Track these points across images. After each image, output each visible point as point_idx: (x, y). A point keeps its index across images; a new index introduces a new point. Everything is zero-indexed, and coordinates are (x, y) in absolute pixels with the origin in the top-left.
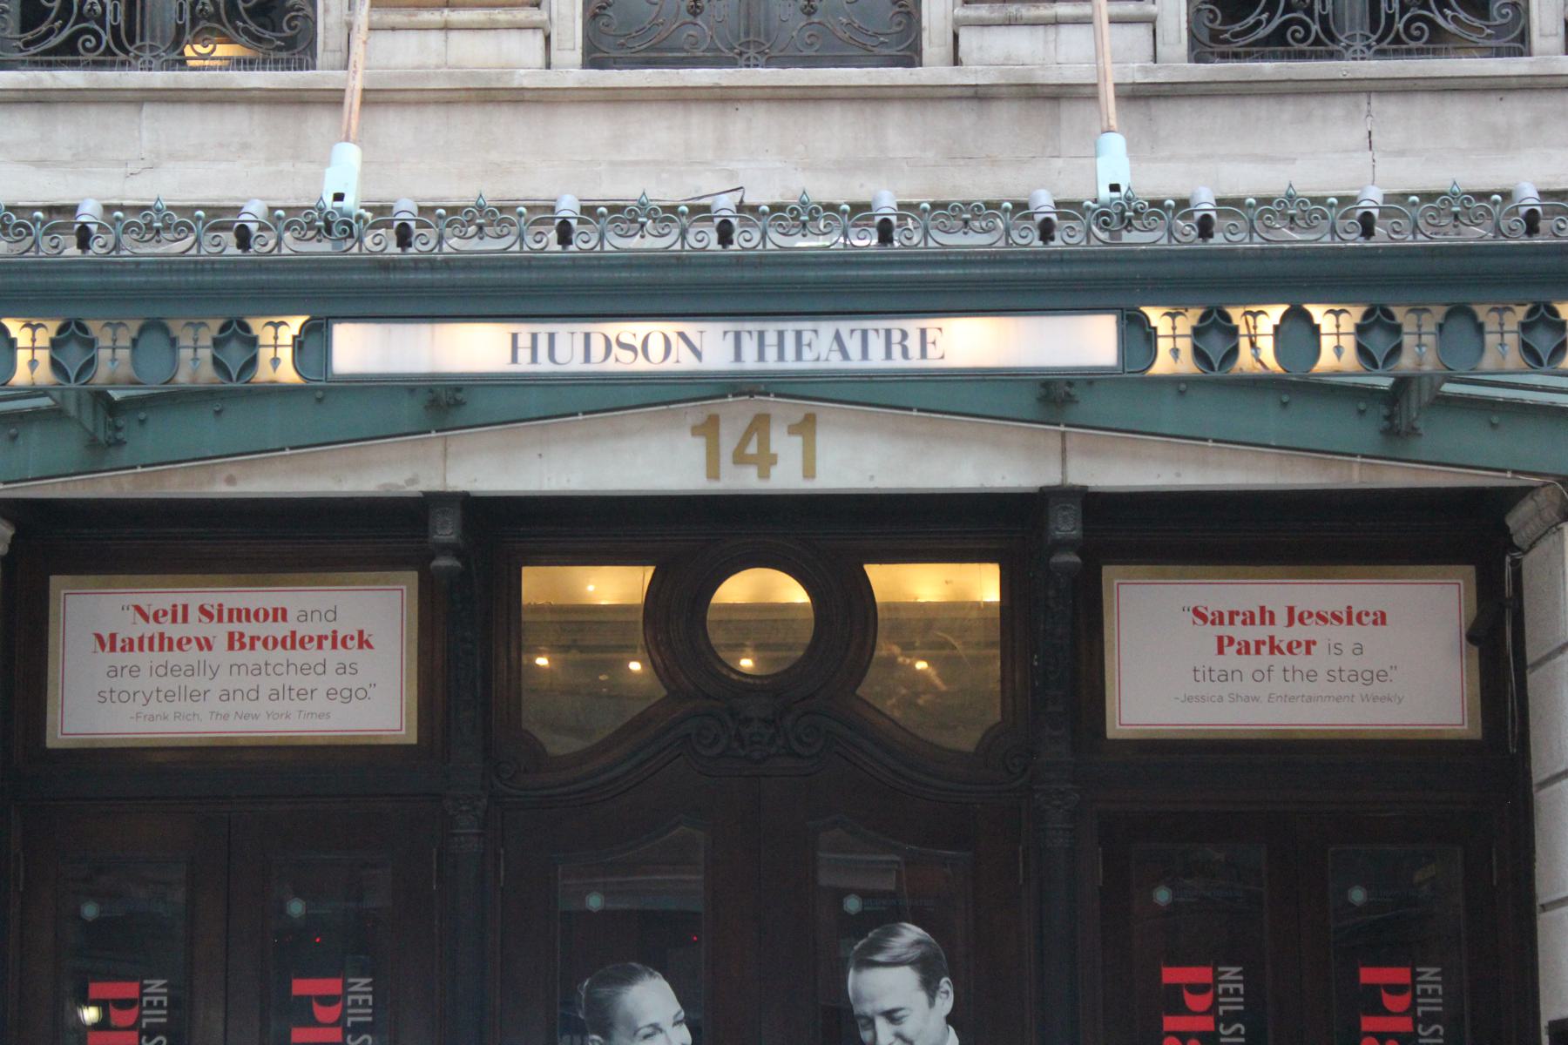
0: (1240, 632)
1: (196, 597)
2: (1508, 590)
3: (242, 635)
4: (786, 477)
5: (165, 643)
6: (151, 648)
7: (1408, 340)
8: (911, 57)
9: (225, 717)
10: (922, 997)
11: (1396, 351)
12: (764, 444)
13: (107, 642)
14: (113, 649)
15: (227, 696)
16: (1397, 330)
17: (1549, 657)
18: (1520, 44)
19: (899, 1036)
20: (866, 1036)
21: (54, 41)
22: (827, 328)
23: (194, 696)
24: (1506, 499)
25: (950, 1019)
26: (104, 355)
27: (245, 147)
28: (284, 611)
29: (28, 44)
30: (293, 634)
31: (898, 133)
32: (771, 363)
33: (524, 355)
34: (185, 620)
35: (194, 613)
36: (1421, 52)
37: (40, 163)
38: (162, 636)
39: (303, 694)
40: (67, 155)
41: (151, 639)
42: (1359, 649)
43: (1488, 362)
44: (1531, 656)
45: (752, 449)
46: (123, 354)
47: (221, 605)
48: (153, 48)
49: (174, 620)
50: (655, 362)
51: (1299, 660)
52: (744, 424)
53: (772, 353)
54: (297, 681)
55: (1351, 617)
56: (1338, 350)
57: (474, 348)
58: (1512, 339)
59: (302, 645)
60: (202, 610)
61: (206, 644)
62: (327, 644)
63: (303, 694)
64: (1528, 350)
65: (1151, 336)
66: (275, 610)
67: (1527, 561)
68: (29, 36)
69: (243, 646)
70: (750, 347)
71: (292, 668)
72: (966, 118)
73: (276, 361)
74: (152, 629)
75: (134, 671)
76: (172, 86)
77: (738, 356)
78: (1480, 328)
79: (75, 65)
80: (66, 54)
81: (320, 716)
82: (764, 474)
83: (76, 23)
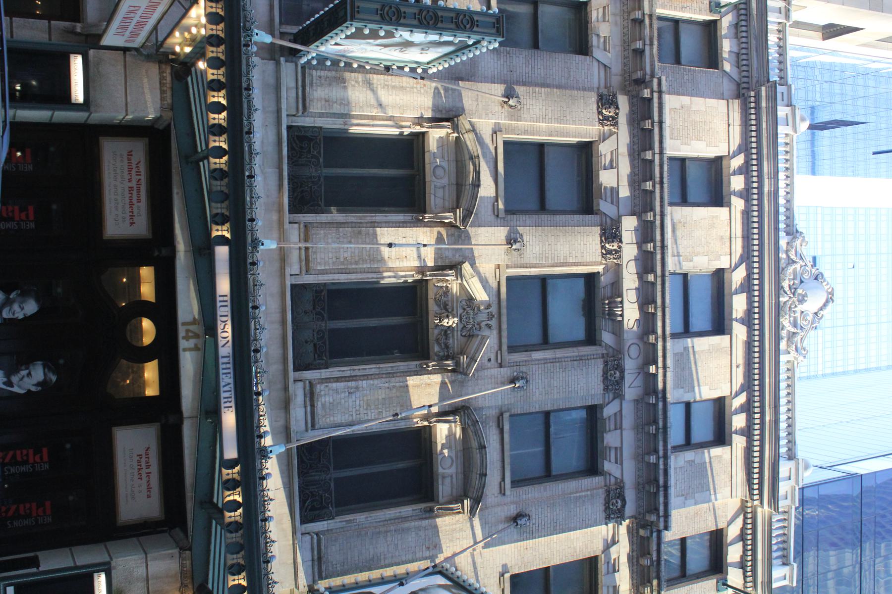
0: (143, 460)
1: (143, 178)
2: (159, 529)
4: (183, 344)
5: (130, 169)
7: (234, 535)
8: (296, 369)
10: (35, 382)
11: (231, 532)
12: (192, 337)
13: (130, 154)
15: (116, 186)
16: (237, 532)
17: (141, 544)
18: (303, 522)
19: (23, 377)
20: (23, 368)
21: (294, 145)
22: (231, 381)
24: (185, 530)
25: (29, 391)
26: (218, 183)
27: (268, 196)
31: (275, 369)
32: (221, 366)
33: (221, 299)
35: (139, 177)
36: (300, 498)
37: (262, 142)
39: (116, 208)
42: (140, 492)
43: (229, 556)
44: (141, 538)
45: (190, 334)
46: (219, 188)
50: (221, 335)
51: (136, 476)
52: (197, 331)
53: (224, 366)
55: (149, 489)
56: (231, 517)
57: (223, 286)
58: (235, 561)
63: (116, 208)
64: (232, 566)
65: (233, 467)
67: (167, 534)
70: (226, 360)
72: (279, 386)
73: (218, 230)
74: (134, 166)
75: (122, 161)
77: (223, 357)
78: (238, 553)
79: (288, 151)
80: (290, 148)
82: (184, 338)
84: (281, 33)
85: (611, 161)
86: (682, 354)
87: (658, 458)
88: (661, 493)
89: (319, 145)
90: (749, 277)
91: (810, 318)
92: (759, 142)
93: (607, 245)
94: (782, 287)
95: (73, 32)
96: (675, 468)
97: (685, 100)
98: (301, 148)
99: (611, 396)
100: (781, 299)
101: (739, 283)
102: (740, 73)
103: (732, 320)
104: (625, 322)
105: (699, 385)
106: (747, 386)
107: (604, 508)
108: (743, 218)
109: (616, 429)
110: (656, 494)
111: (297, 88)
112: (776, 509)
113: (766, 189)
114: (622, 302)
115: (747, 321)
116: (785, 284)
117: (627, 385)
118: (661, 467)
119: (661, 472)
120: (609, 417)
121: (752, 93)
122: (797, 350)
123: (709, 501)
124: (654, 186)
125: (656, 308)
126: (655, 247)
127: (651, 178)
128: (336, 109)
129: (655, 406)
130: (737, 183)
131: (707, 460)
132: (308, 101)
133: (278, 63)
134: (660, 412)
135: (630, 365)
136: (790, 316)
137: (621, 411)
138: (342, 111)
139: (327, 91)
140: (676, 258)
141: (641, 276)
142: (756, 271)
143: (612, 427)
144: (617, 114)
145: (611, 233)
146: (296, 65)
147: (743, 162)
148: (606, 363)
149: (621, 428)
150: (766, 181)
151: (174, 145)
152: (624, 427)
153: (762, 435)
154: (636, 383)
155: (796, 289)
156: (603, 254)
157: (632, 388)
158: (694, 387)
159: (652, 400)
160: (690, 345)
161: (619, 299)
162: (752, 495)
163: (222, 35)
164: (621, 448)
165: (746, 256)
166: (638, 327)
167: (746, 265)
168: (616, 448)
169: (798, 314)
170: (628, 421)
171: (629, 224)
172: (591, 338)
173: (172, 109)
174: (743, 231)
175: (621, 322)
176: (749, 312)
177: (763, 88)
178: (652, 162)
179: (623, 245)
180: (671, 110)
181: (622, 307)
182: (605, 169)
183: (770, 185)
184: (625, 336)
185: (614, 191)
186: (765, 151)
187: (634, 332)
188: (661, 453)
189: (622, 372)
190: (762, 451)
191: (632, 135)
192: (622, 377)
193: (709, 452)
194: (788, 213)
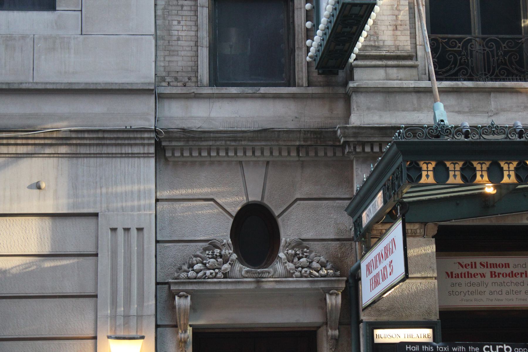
1: (478, 260)
3: (495, 272)
6: (465, 277)
9: (492, 300)
14: (452, 277)
15: (491, 293)
23: (481, 293)
28: (508, 264)
29: (444, 73)
30: (512, 272)
34: (475, 267)
35: (478, 265)
37: (459, 112)
38: (468, 272)
39: (517, 292)
40: (467, 110)
41: (465, 274)
47: (487, 262)
48: (485, 75)
49: (472, 267)
54: (515, 288)
59: (516, 276)
60: (481, 264)
61: (483, 276)
62: (524, 275)
63: (517, 292)
66: (505, 264)
68: (444, 70)
69: (496, 276)
71: (513, 284)
74: (465, 270)
75: (460, 285)
76: (502, 87)
81: (523, 300)
83: (507, 66)
84: (310, 84)
89: (450, 39)
95: (336, 340)
98: (455, 63)
111: (386, 66)
128: (404, 15)
132: (399, 53)
133: (357, 90)
138: (407, 8)
139: (383, 28)
146: (358, 66)
151: (454, 223)
163: (461, 164)
173: (425, 224)
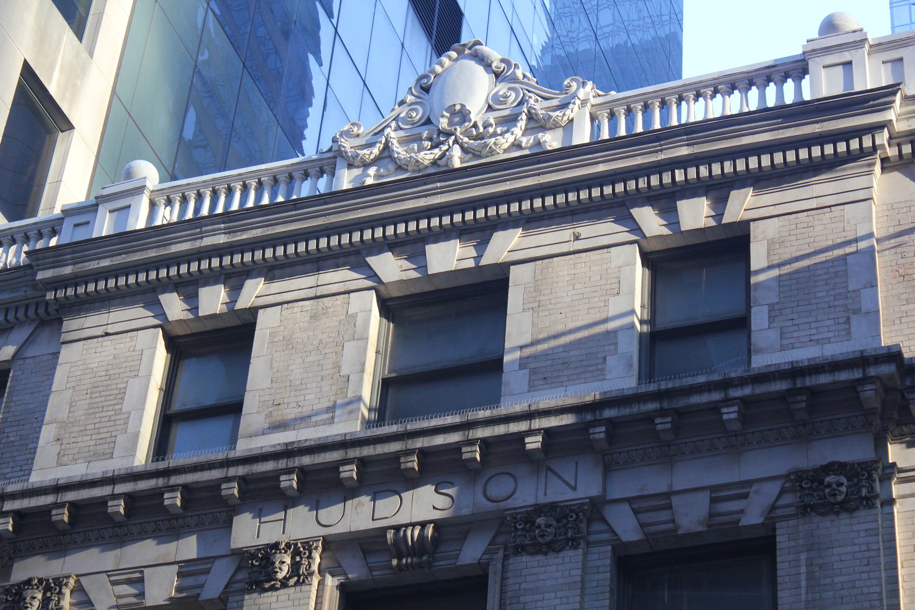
85: (129, 582)
86: (533, 372)
87: (727, 402)
88: (809, 382)
90: (393, 245)
91: (502, 88)
92: (136, 268)
93: (280, 576)
94: (434, 163)
96: (782, 348)
97: (47, 433)
99: (597, 526)
100: (457, 164)
101: (407, 264)
102: (19, 323)
103: (478, 269)
104: (437, 515)
105: (606, 321)
106: (619, 209)
107: (843, 515)
108: (282, 277)
109: (669, 507)
110: (814, 393)
112: (891, 90)
113: (222, 239)
114: (397, 528)
115: (479, 234)
116: (427, 157)
117: (569, 495)
118: (747, 391)
119: (760, 389)
120: (642, 526)
121: (50, 296)
122: (564, 106)
123: (871, 251)
124: (172, 489)
125: (408, 452)
126: (289, 471)
127: (157, 494)
129: (611, 423)
130: (214, 300)
131: (775, 273)
134: (626, 411)
135: (527, 493)
136: (495, 135)
137: (629, 500)
140: (338, 412)
141: (348, 492)
142: (379, 233)
143: (664, 516)
144: (40, 581)
145: (257, 570)
147: (175, 294)
148: (520, 550)
149: (668, 495)
150: (208, 241)
152: (663, 488)
153: (721, 156)
154: (569, 477)
155: (440, 132)
156: (297, 583)
157: (578, 483)
158: (608, 333)
159: (599, 433)
160: (517, 355)
161: (390, 535)
162: (862, 153)
164: (713, 489)
165: (353, 259)
166: (452, 484)
167: (371, 254)
168: (713, 501)
169: (491, 118)
170: (651, 481)
171: (248, 531)
172: (474, 584)
174: (305, 273)
175: (438, 525)
176: (462, 232)
177: (40, 276)
178: (130, 498)
179: (284, 540)
180: (59, 464)
181: (406, 526)
182: (141, 595)
183: (214, 233)
184: (465, 511)
185: (187, 569)
186: (152, 253)
187: (460, 493)
188: (716, 396)
189: (539, 509)
190: (757, 150)
191: (85, 544)
192: (551, 508)
193: (758, 272)
194: (312, 171)
